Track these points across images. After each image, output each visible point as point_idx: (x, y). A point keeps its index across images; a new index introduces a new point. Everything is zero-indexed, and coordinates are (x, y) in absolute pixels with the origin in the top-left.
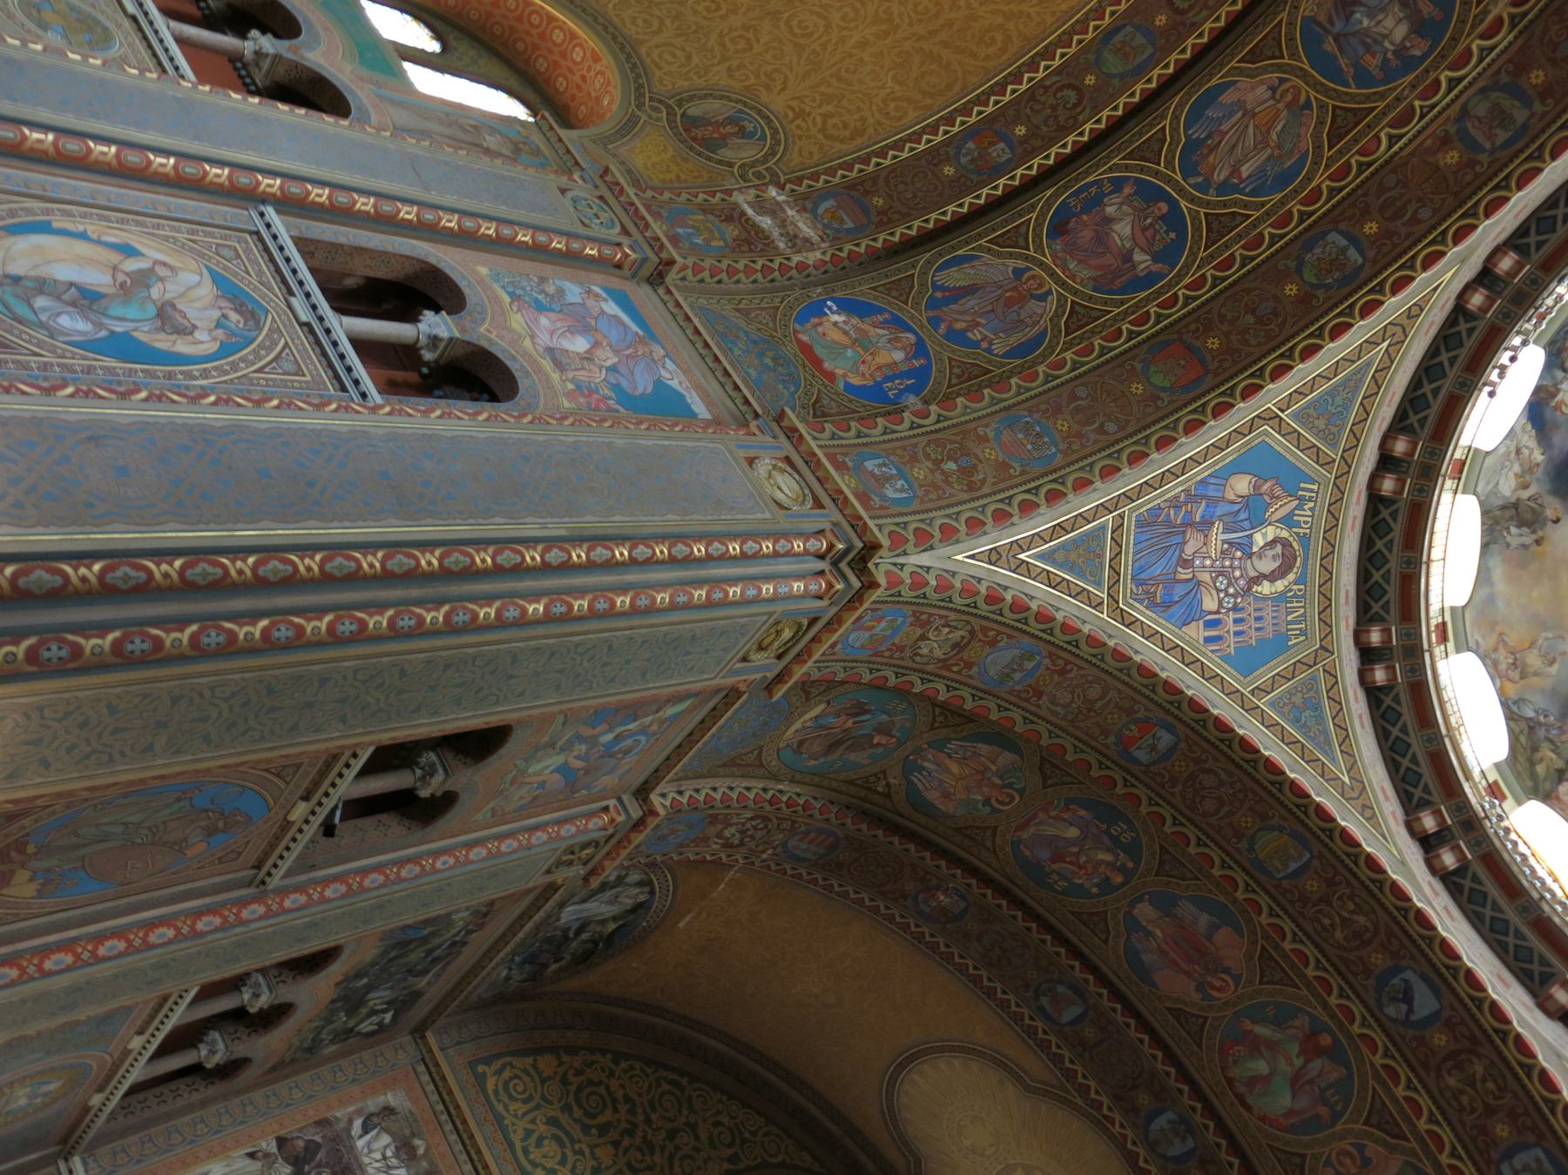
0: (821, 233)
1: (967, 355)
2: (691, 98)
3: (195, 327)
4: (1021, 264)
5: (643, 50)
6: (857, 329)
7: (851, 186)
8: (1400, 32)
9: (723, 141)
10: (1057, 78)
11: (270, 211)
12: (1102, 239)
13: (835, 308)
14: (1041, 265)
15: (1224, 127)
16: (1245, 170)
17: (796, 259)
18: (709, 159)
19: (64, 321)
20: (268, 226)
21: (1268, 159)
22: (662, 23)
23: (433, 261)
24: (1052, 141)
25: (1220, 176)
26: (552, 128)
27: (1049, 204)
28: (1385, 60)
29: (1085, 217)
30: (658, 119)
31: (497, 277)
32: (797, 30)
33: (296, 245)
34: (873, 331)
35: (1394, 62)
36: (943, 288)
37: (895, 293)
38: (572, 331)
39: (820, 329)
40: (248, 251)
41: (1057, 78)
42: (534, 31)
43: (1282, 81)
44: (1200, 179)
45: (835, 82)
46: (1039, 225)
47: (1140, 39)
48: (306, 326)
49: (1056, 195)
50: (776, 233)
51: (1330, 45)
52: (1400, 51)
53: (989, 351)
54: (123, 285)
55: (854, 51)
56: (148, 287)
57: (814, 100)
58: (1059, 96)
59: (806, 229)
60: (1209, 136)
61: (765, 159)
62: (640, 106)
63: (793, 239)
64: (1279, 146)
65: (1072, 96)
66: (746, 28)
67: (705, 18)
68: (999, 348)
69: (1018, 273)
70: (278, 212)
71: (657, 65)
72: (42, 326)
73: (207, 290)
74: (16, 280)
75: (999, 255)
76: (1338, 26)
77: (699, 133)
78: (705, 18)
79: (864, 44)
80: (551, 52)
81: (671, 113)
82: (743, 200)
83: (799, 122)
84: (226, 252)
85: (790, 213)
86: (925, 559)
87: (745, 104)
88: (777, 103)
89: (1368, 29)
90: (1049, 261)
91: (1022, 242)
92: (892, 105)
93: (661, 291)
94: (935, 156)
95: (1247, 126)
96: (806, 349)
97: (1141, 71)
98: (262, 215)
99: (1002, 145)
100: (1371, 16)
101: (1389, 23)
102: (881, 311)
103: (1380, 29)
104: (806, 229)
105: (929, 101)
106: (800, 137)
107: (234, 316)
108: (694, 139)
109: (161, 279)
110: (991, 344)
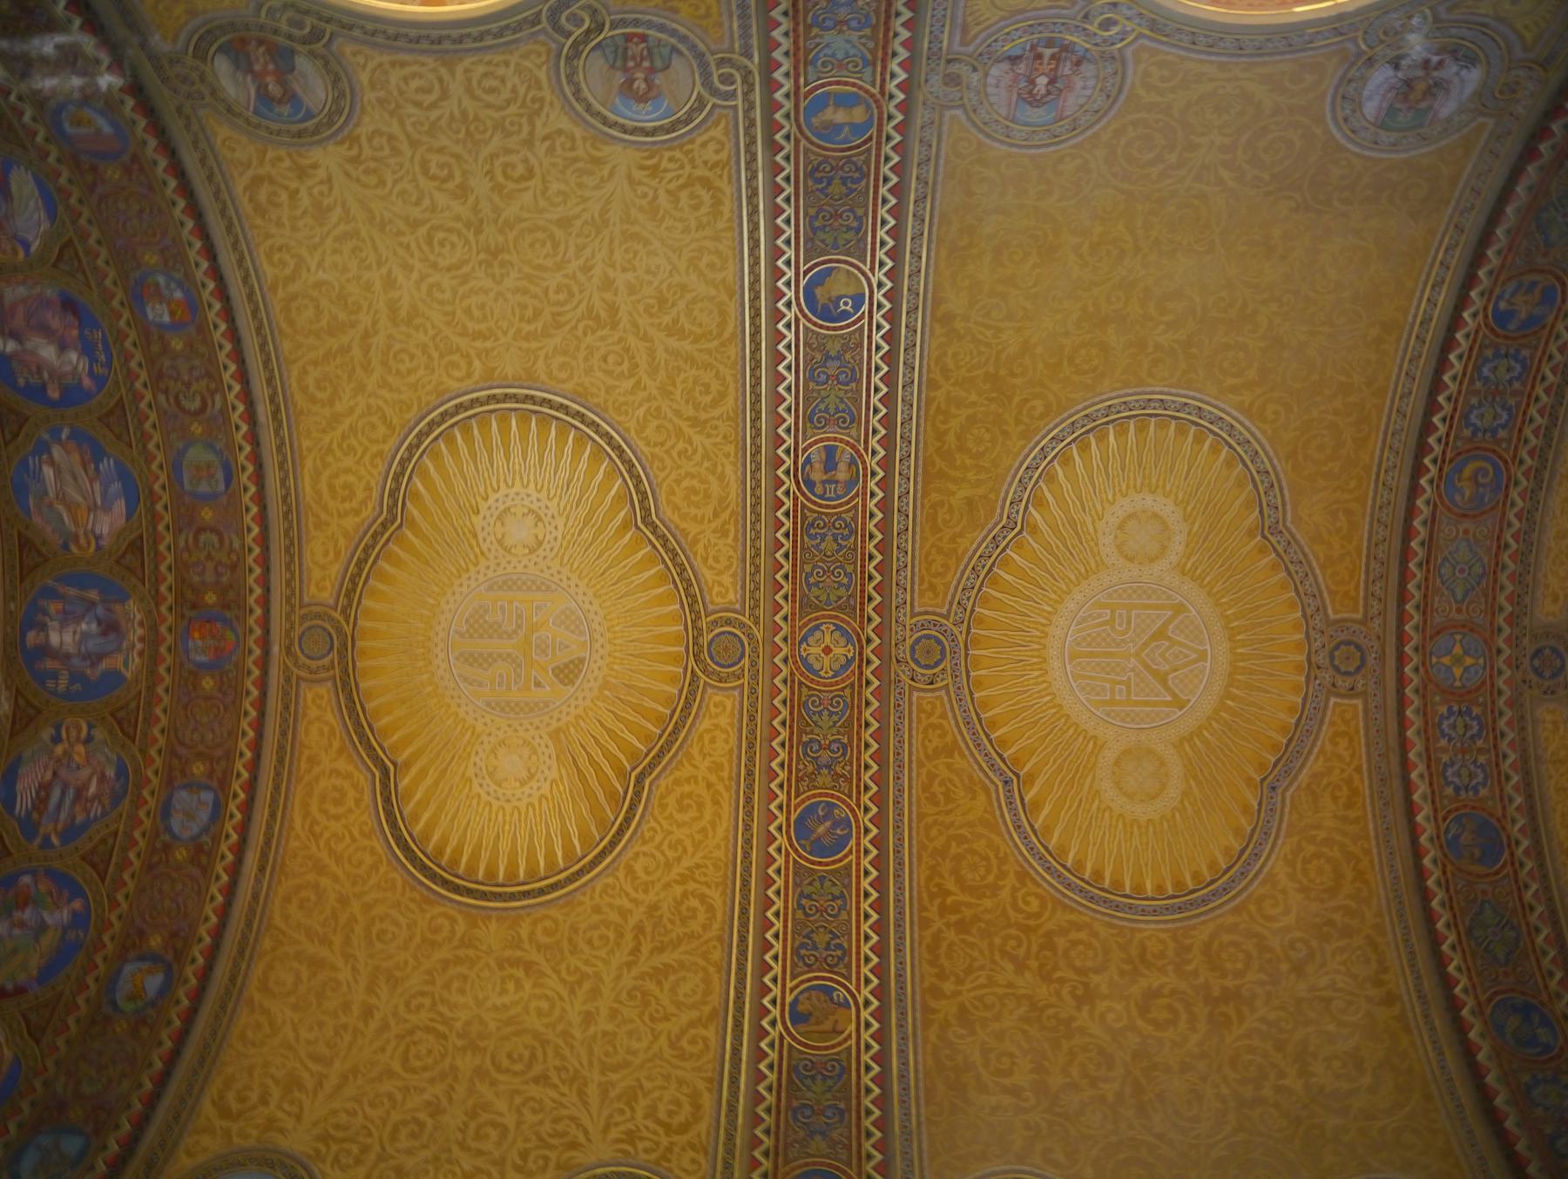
8: (54, 639)
10: (218, 405)
12: (46, 331)
15: (97, 486)
16: (48, 472)
21: (46, 493)
25: (57, 452)
28: (45, 613)
35: (40, 617)
41: (218, 405)
43: (98, 548)
44: (64, 436)
45: (343, 228)
47: (204, 488)
51: (93, 595)
52: (43, 627)
55: (384, 270)
60: (97, 469)
64: (51, 505)
65: (196, 405)
69: (26, 246)
76: (100, 610)
79: (390, 283)
89: (78, 623)
95: (85, 498)
100: (86, 636)
101: (68, 638)
103: (71, 629)
105: (281, 294)
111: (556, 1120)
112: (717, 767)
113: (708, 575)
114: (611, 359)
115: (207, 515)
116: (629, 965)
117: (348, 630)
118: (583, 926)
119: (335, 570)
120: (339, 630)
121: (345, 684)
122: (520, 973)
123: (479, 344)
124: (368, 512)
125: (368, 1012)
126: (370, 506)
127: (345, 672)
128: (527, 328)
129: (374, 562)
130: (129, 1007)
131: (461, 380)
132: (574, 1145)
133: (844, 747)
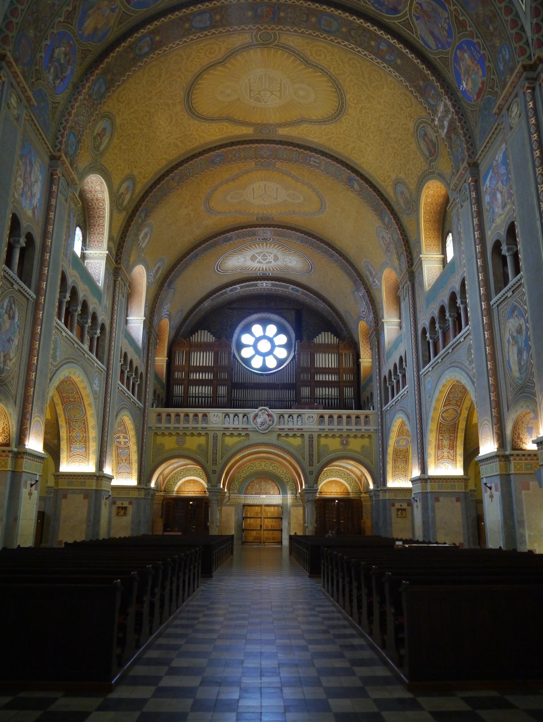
0: (440, 101)
1: (454, 27)
2: (424, 155)
3: (520, 324)
4: (414, 19)
5: (419, 174)
6: (464, 76)
7: (421, 94)
9: (431, 141)
11: (492, 303)
13: (462, 86)
14: (410, 10)
17: (452, 110)
18: (438, 145)
19: (525, 358)
20: (494, 303)
22: (409, 170)
23: (491, 250)
24: (370, 31)
26: (450, 206)
27: (390, 18)
29: (386, 3)
30: (435, 165)
31: (490, 228)
32: (388, 126)
33: (498, 294)
34: (463, 69)
36: (437, 45)
37: (447, 63)
38: (496, 200)
39: (470, 91)
40: (502, 308)
41: (351, 41)
42: (432, 207)
46: (398, 18)
47: (323, 22)
48: (513, 292)
49: (385, 17)
50: (447, 119)
53: (448, 18)
54: (515, 343)
56: (514, 336)
57: (404, 113)
58: (355, 37)
59: (441, 108)
61: (429, 124)
62: (434, 172)
63: (447, 111)
65: (353, 32)
66: (396, 142)
67: (400, 156)
68: (446, 15)
69: (418, 18)
70: (491, 300)
71: (421, 169)
72: (527, 363)
73: (511, 320)
74: (520, 369)
75: (415, 28)
77: (433, 150)
78: (400, 156)
79: (379, 103)
80: (435, 200)
81: (432, 161)
82: (444, 133)
83: (413, 116)
84: (503, 315)
85: (439, 115)
86: (528, 28)
87: (417, 136)
88: (411, 125)
90: (407, 8)
91: (407, 22)
92: (391, 86)
93: (479, 162)
94: (397, 68)
96: (478, 95)
97: (332, 16)
98: (493, 305)
99: (381, 47)
102: (455, 67)
104: (441, 108)
105: (383, 75)
106: (417, 114)
107: (516, 313)
108: (435, 151)
109: (512, 333)
110: (446, 19)
111: (139, 159)
112: (231, 132)
113: (287, 129)
114: (349, 133)
115: (314, 20)
116: (176, 139)
117: (271, 46)
118: (184, 125)
119: (292, 44)
120: (270, 43)
121: (251, 46)
122: (169, 121)
123: (358, 109)
124: (311, 58)
125: (150, 99)
126: (314, 60)
127: (255, 45)
128: (361, 122)
129: (294, 55)
130: (137, 52)
131: (349, 98)
132: (135, 167)
133: (240, 157)
